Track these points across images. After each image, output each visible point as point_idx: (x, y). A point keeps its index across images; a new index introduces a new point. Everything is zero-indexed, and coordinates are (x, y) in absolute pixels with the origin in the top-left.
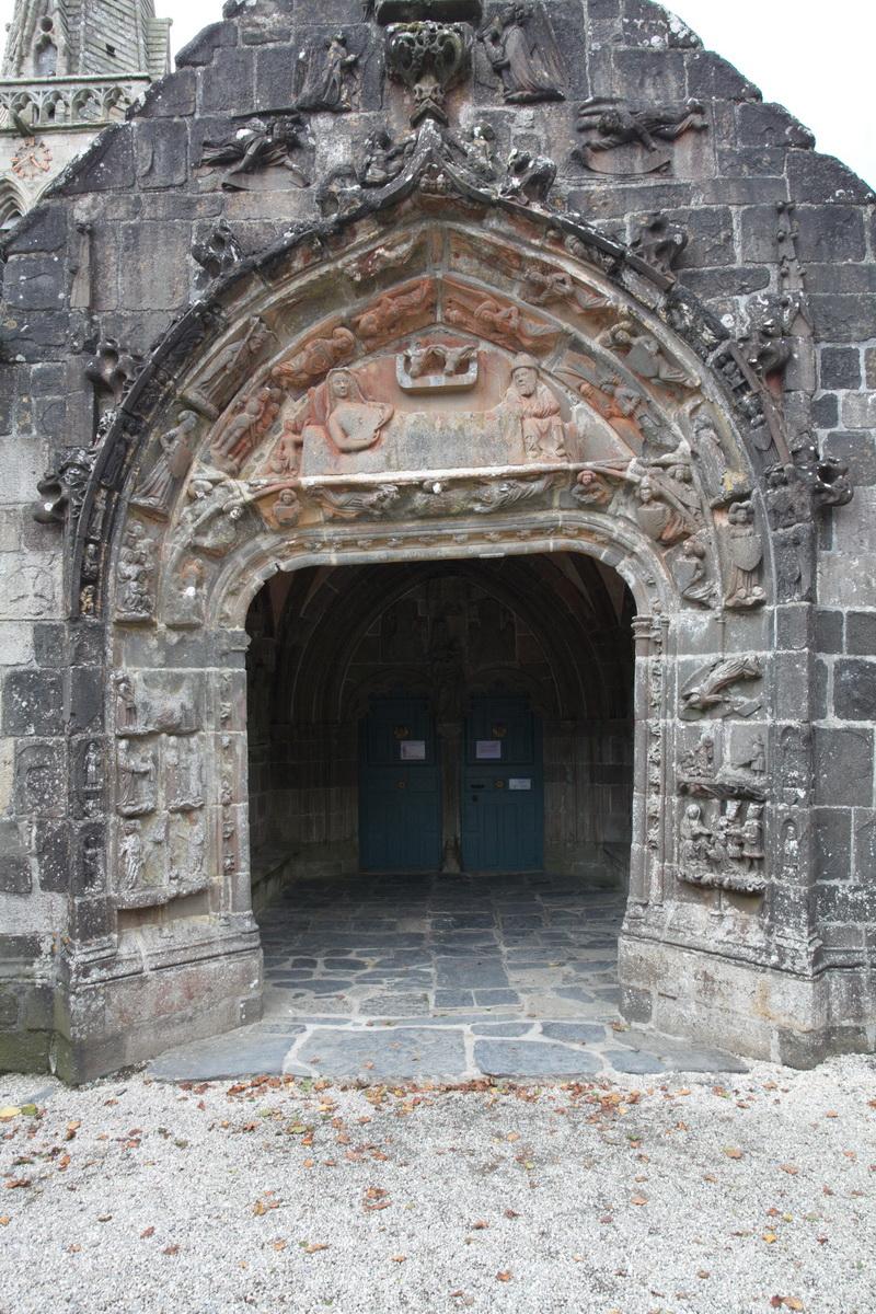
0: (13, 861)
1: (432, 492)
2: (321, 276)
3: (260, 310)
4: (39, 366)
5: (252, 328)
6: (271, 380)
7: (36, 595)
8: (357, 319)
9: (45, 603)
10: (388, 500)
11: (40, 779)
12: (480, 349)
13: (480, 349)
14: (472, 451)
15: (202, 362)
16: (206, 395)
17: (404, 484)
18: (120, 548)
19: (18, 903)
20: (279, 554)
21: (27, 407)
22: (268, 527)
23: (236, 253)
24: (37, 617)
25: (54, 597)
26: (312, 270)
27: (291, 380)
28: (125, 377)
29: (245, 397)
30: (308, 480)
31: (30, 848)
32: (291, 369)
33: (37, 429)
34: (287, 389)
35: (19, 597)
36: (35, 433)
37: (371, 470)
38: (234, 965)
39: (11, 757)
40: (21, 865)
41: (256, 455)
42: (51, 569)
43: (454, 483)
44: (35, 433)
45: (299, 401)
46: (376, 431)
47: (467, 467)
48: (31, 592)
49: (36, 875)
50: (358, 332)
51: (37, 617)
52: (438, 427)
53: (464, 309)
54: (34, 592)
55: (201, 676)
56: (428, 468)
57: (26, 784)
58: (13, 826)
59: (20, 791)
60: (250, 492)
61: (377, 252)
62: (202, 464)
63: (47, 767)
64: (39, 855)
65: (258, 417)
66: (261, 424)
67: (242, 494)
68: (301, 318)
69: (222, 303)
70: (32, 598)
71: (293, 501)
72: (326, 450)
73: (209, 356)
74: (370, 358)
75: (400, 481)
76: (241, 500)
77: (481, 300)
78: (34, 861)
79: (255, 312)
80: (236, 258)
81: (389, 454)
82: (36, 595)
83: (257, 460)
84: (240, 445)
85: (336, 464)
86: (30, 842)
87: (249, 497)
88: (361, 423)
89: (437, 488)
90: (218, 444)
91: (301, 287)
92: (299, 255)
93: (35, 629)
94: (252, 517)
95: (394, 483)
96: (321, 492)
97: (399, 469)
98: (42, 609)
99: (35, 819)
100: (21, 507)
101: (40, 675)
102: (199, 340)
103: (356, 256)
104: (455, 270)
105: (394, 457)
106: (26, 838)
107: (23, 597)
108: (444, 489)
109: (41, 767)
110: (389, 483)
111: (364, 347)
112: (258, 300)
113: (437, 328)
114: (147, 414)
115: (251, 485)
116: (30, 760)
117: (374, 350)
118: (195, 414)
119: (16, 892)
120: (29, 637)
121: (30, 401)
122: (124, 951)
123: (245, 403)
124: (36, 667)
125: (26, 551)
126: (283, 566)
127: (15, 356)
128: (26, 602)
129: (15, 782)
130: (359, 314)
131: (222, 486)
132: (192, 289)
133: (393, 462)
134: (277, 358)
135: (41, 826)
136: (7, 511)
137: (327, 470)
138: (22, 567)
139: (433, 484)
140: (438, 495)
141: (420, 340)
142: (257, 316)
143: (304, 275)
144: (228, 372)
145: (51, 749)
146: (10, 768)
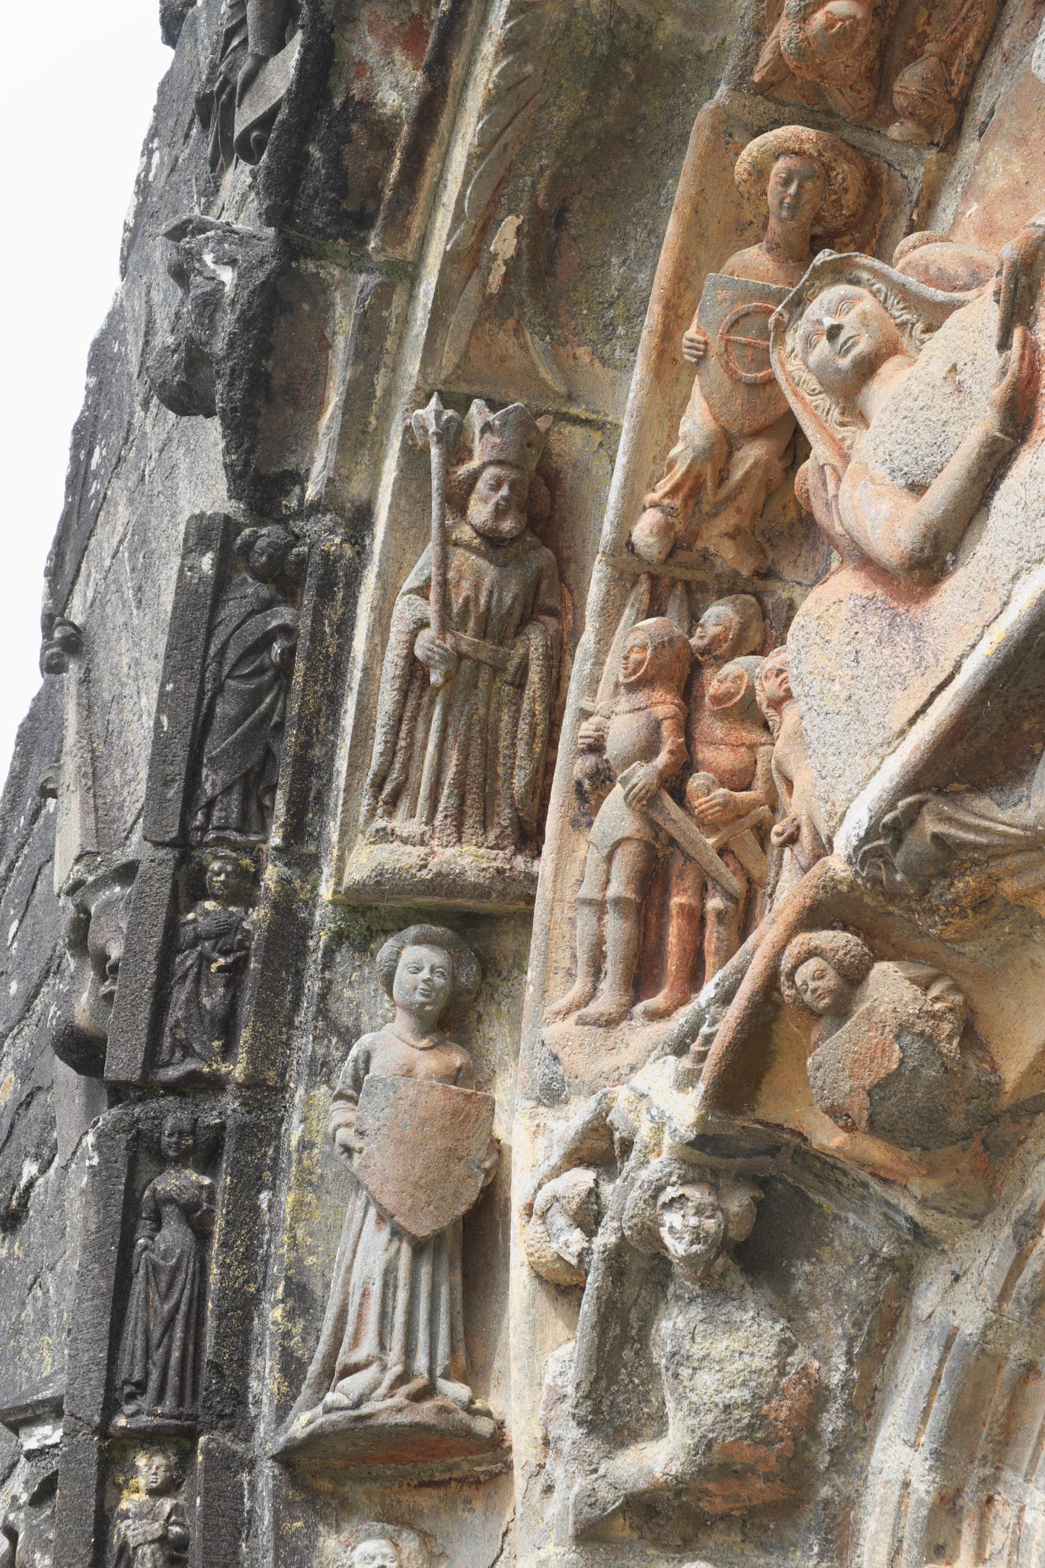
2: (507, 47)
3: (413, 366)
5: (434, 451)
8: (766, 55)
15: (348, 721)
16: (414, 827)
22: (911, 1209)
26: (471, 63)
27: (728, 520)
29: (587, 728)
32: (679, 470)
34: (767, 574)
46: (1004, 344)
50: (842, 102)
65: (662, 759)
66: (697, 781)
68: (617, 272)
69: (291, 462)
73: (356, 675)
74: (970, 147)
76: (667, 1141)
79: (408, 386)
80: (227, 276)
84: (674, 931)
90: (579, 987)
91: (474, 159)
92: (372, 58)
94: (829, 1206)
96: (930, 825)
102: (277, 648)
111: (895, 131)
114: (228, 1052)
117: (963, 104)
118: (413, 931)
123: (596, 747)
130: (760, 32)
134: (613, 495)
142: (429, 397)
143: (460, 102)
144: (435, 678)
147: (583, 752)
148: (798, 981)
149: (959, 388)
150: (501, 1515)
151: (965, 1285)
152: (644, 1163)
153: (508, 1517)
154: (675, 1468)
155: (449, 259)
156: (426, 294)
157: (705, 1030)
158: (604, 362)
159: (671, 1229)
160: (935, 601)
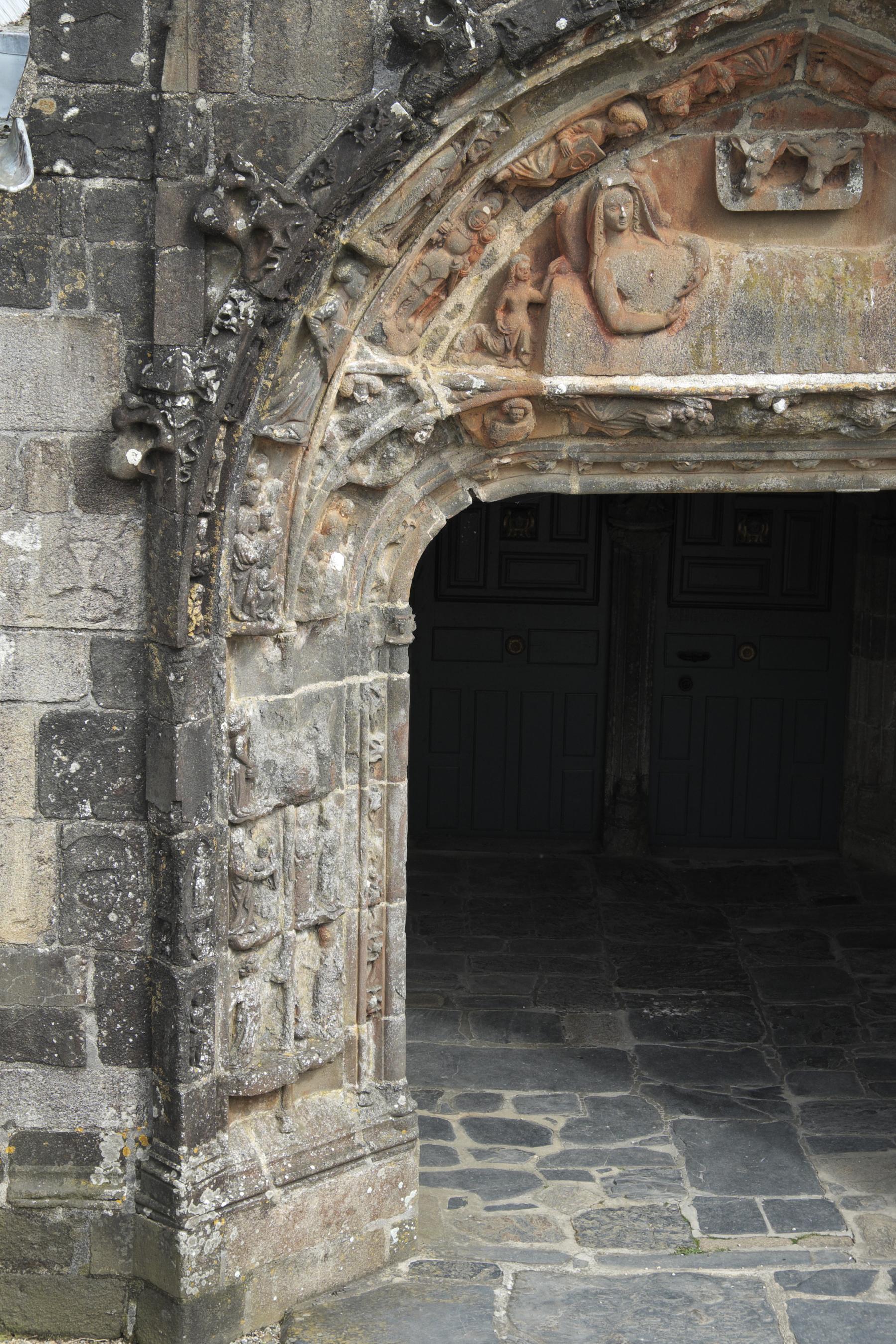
0: (57, 1017)
1: (771, 409)
4: (99, 183)
6: (491, 186)
7: (95, 588)
9: (110, 602)
10: (692, 422)
11: (101, 890)
12: (868, 128)
13: (868, 128)
14: (847, 344)
17: (725, 398)
18: (237, 510)
19: (58, 1080)
20: (476, 477)
21: (79, 263)
23: (475, 36)
24: (96, 626)
25: (126, 594)
28: (271, 238)
29: (446, 225)
30: (561, 384)
31: (84, 997)
33: (97, 302)
35: (65, 590)
36: (91, 307)
37: (665, 370)
38: (384, 1168)
39: (50, 852)
40: (70, 1023)
41: (449, 305)
42: (122, 545)
43: (806, 397)
44: (91, 307)
45: (532, 211)
47: (834, 372)
48: (87, 581)
49: (91, 1039)
51: (96, 626)
52: (787, 295)
53: (846, 70)
54: (91, 581)
55: (338, 692)
56: (766, 372)
57: (76, 896)
58: (57, 962)
59: (66, 908)
60: (451, 400)
61: (712, 13)
62: (364, 343)
63: (114, 871)
64: (99, 1010)
67: (438, 407)
70: (87, 592)
71: (525, 414)
72: (590, 329)
75: (718, 392)
77: (882, 72)
78: (89, 1020)
80: (473, 43)
81: (699, 346)
82: (95, 588)
83: (450, 316)
85: (605, 356)
86: (84, 988)
87: (449, 409)
88: (651, 280)
89: (781, 406)
93: (94, 645)
95: (707, 396)
97: (715, 369)
98: (105, 612)
99: (92, 952)
100: (67, 437)
101: (100, 720)
103: (675, 21)
104: (841, 15)
105: (708, 347)
106: (78, 981)
107: (70, 590)
108: (791, 406)
109: (104, 870)
110: (698, 395)
112: (502, 88)
113: (793, 87)
115: (454, 388)
116: (83, 859)
119: (62, 1064)
120: (82, 659)
121: (83, 249)
122: (236, 1157)
124: (93, 707)
125: (77, 513)
126: (483, 494)
127: (53, 163)
128: (78, 600)
129: (59, 891)
131: (401, 384)
132: (378, 66)
133: (707, 358)
135: (102, 963)
136: (45, 445)
137: (591, 367)
138: (70, 540)
139: (776, 399)
140: (781, 414)
141: (760, 108)
145: (120, 843)
146: (49, 870)
147: (438, 231)
148: (515, 411)
149: (651, 280)
150: (290, 457)
151: (459, 458)
152: (423, 412)
153: (293, 459)
154: (370, 483)
155: (536, 88)
156: (519, 88)
157: (468, 393)
158: (527, 109)
159: (421, 436)
160: (613, 341)
